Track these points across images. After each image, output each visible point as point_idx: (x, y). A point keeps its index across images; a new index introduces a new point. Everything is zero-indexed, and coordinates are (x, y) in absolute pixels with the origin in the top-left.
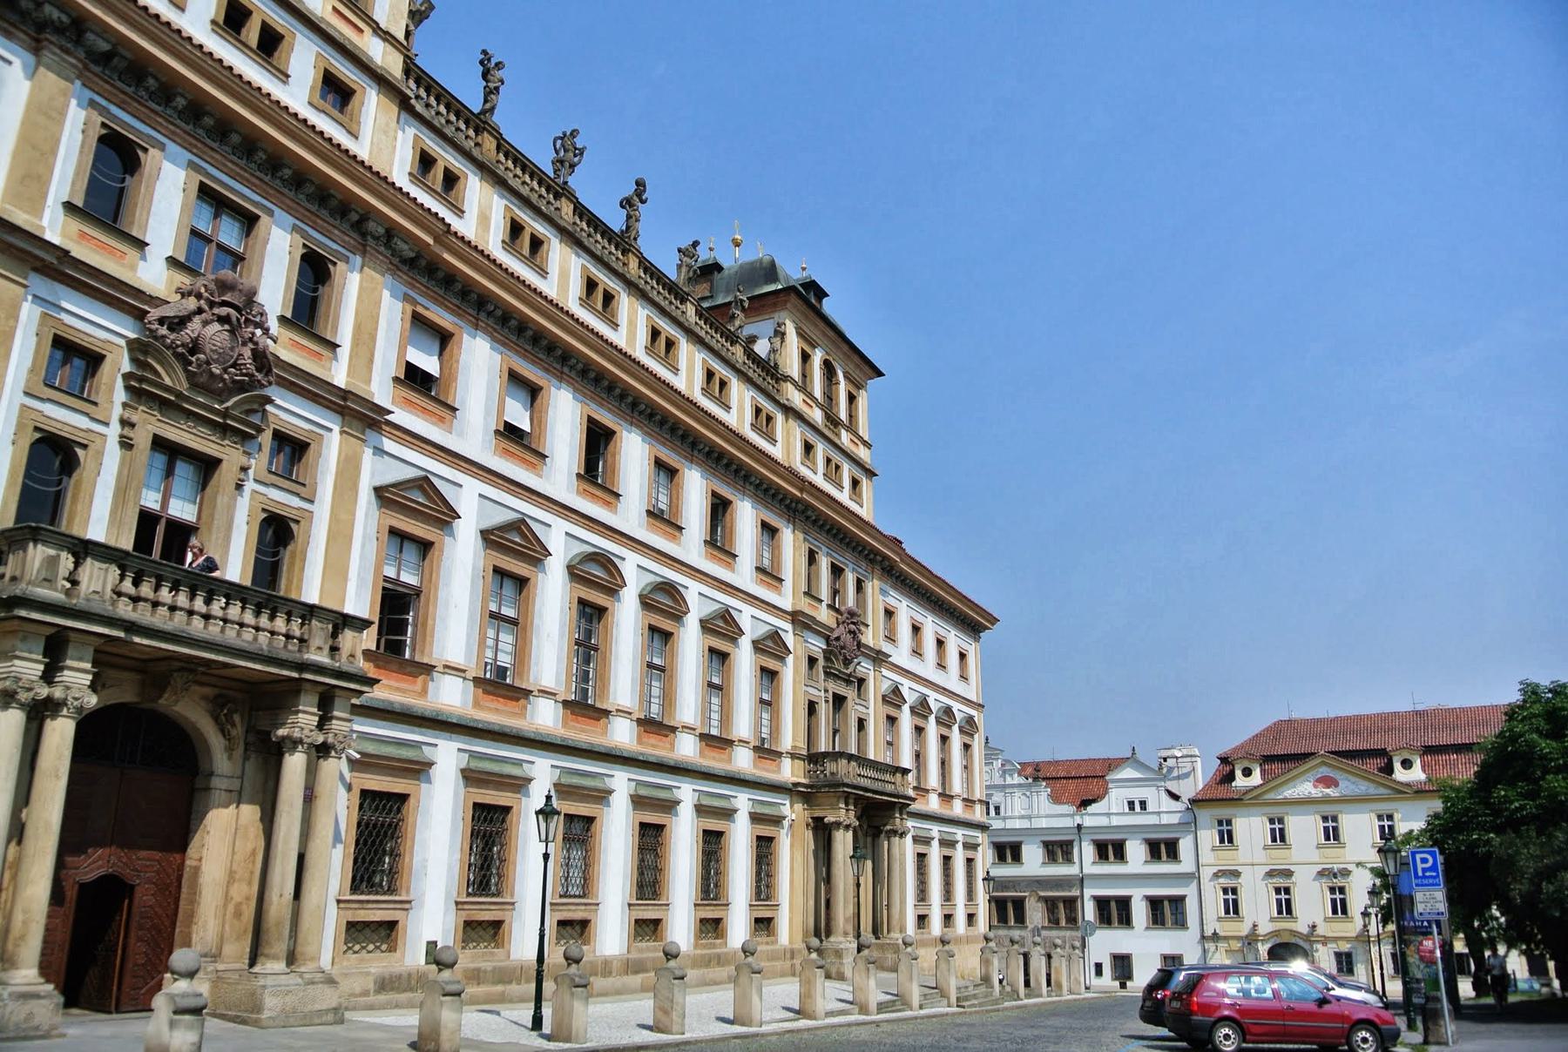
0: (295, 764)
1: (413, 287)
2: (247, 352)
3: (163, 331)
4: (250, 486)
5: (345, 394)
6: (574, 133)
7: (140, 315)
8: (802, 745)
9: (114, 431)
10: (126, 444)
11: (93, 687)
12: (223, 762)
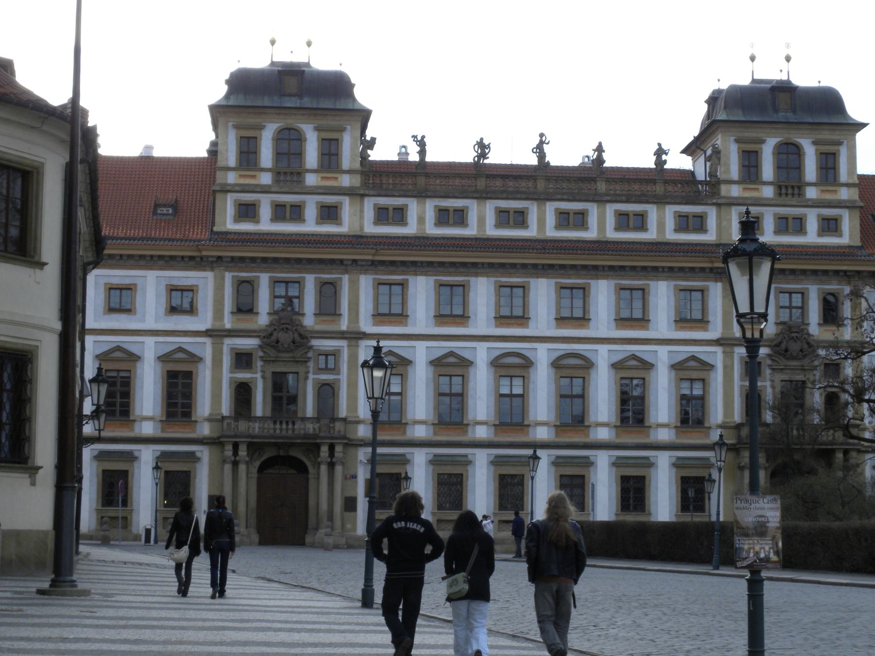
0: (324, 468)
1: (377, 274)
2: (296, 335)
3: (265, 340)
4: (311, 376)
5: (343, 333)
6: (482, 139)
7: (258, 337)
8: (738, 416)
9: (259, 375)
10: (263, 377)
11: (248, 455)
12: (311, 470)
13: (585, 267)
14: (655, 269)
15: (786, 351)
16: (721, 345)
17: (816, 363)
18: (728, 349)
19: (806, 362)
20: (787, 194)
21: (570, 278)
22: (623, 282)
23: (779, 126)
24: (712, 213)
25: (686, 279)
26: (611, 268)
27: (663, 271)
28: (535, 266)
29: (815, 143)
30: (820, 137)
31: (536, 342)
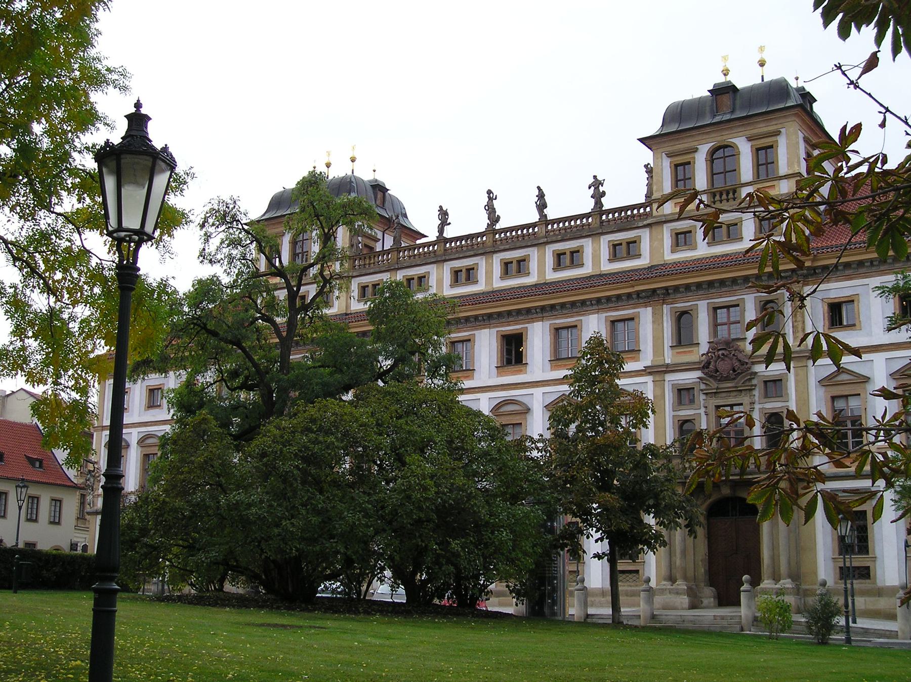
6: (441, 207)
13: (519, 312)
14: (583, 302)
15: (717, 371)
16: (650, 374)
17: (754, 382)
18: (658, 378)
19: (740, 381)
20: (728, 200)
21: (509, 325)
22: (557, 321)
23: (708, 130)
24: (645, 236)
25: (616, 309)
26: (543, 309)
27: (592, 305)
28: (476, 317)
29: (750, 139)
30: (755, 131)
31: (478, 392)
